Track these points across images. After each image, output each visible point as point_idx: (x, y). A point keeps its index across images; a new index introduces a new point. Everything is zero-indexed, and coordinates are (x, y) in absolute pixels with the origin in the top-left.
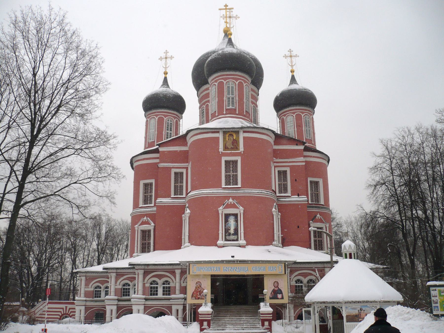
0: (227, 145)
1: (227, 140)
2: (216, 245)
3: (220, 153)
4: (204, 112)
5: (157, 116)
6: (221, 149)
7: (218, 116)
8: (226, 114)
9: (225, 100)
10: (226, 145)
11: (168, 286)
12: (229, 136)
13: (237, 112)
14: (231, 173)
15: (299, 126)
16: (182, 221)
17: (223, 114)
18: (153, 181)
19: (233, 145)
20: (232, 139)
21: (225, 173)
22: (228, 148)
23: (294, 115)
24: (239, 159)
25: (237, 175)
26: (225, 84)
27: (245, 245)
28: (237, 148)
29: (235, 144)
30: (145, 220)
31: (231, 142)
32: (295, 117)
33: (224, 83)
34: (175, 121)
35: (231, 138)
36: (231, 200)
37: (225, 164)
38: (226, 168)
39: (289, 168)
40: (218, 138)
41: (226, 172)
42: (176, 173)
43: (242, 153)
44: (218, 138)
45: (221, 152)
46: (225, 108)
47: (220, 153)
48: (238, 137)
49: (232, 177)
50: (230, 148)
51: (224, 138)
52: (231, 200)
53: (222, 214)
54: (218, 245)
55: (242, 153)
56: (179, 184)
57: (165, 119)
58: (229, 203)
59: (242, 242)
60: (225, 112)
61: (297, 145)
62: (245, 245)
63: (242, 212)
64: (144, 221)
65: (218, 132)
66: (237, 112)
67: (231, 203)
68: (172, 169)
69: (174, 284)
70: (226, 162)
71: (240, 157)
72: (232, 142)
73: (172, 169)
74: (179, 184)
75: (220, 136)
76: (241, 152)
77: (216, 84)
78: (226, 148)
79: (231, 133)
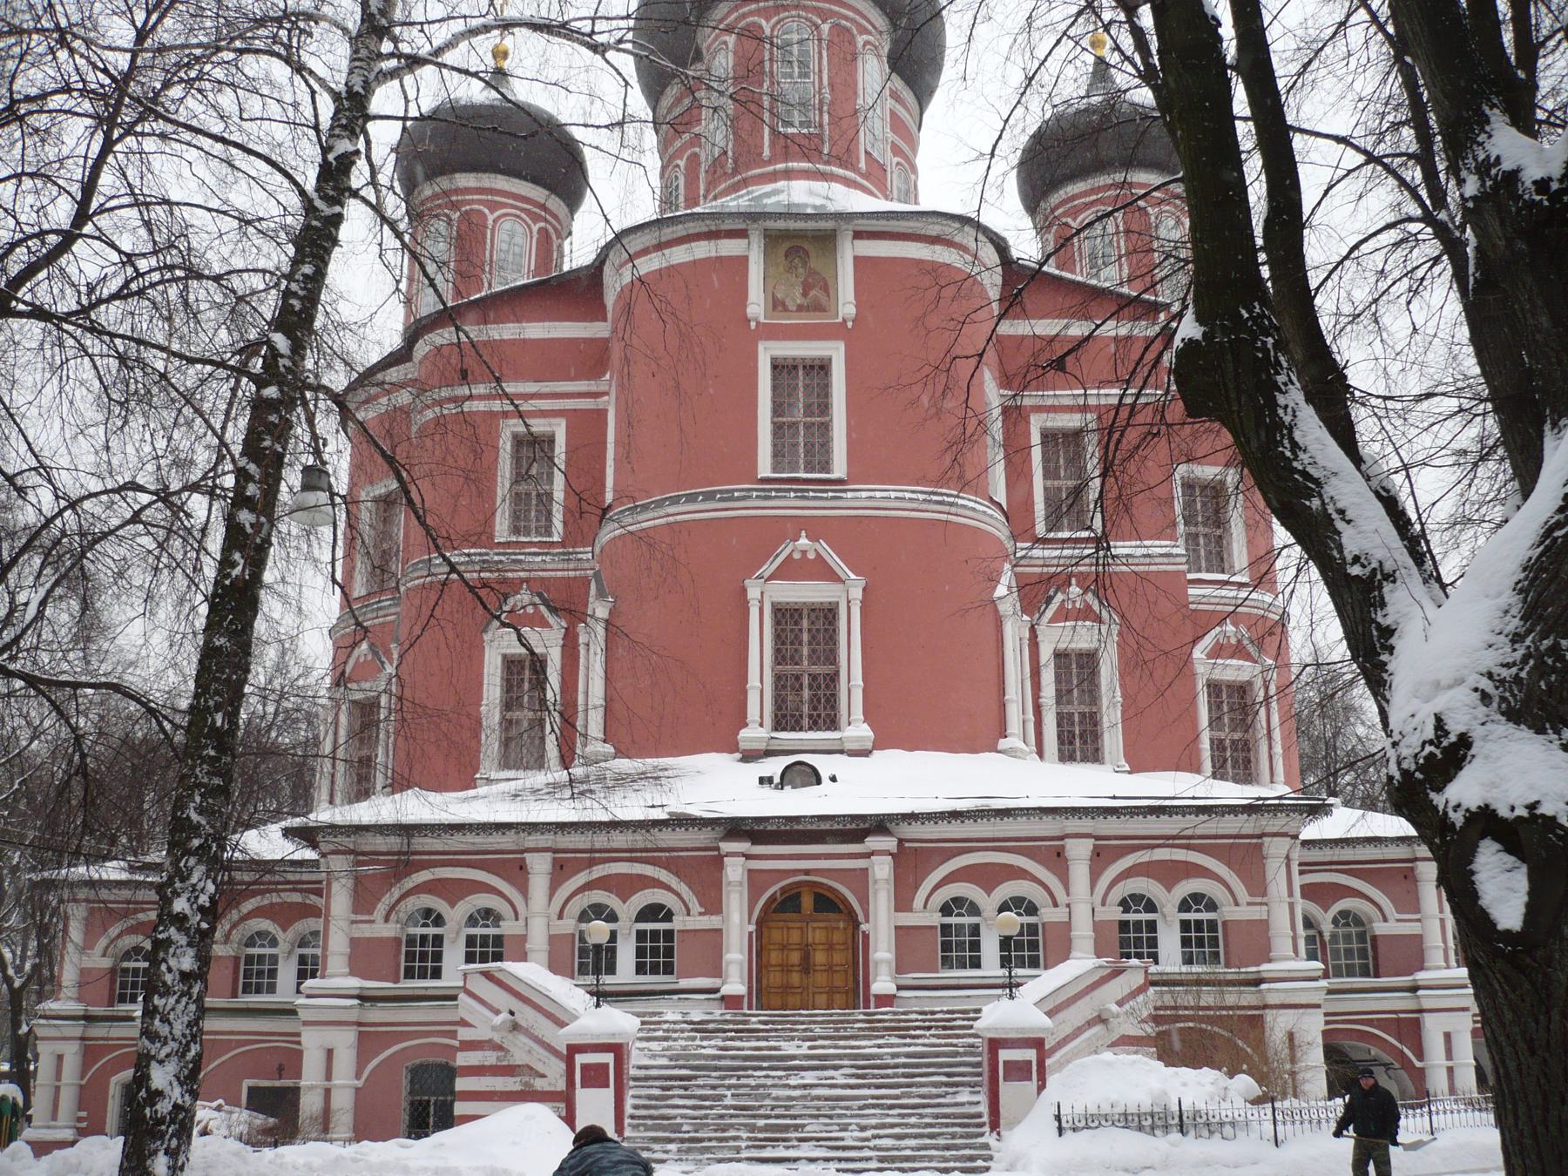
2: (730, 746)
3: (753, 325)
6: (756, 305)
11: (491, 931)
21: (773, 417)
24: (836, 352)
27: (869, 745)
36: (803, 541)
37: (774, 378)
38: (775, 388)
41: (777, 409)
43: (850, 324)
45: (758, 323)
47: (753, 325)
52: (803, 541)
53: (761, 602)
54: (742, 746)
55: (850, 324)
58: (797, 556)
59: (858, 730)
62: (869, 745)
63: (857, 593)
65: (742, 234)
69: (521, 922)
70: (778, 367)
71: (841, 346)
75: (754, 252)
76: (845, 321)
78: (776, 305)
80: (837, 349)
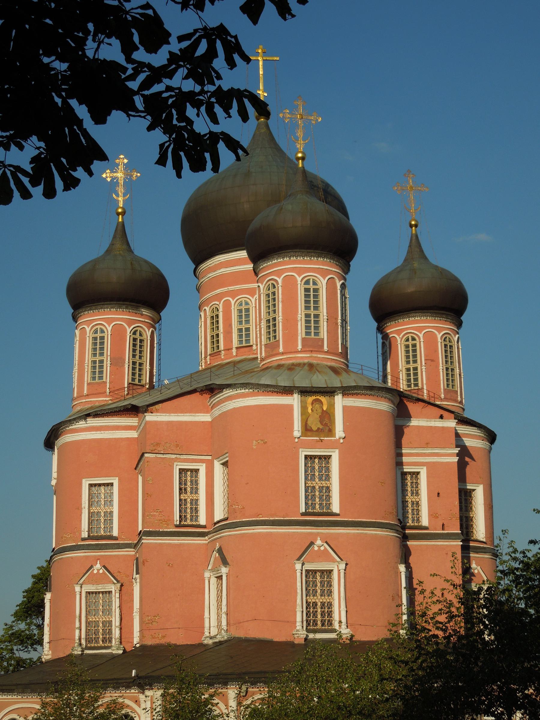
0: (309, 422)
1: (310, 411)
4: (217, 316)
5: (109, 321)
7: (283, 354)
8: (301, 352)
9: (299, 319)
10: (306, 424)
12: (312, 404)
13: (326, 348)
14: (317, 483)
15: (432, 361)
16: (204, 580)
17: (297, 352)
18: (115, 481)
19: (321, 422)
20: (320, 411)
22: (311, 430)
23: (421, 336)
25: (328, 489)
26: (299, 282)
28: (331, 432)
29: (326, 421)
30: (98, 570)
31: (318, 416)
32: (422, 340)
33: (297, 281)
34: (149, 334)
35: (317, 406)
39: (425, 468)
40: (290, 408)
42: (181, 471)
44: (290, 408)
46: (300, 338)
48: (332, 406)
49: (320, 491)
50: (315, 428)
51: (304, 408)
56: (188, 497)
57: (129, 330)
60: (300, 347)
61: (441, 417)
64: (95, 572)
66: (326, 348)
67: (319, 547)
68: (175, 464)
72: (320, 417)
73: (175, 464)
74: (188, 497)
77: (280, 281)
78: (306, 429)
79: (320, 398)
80: (334, 452)
